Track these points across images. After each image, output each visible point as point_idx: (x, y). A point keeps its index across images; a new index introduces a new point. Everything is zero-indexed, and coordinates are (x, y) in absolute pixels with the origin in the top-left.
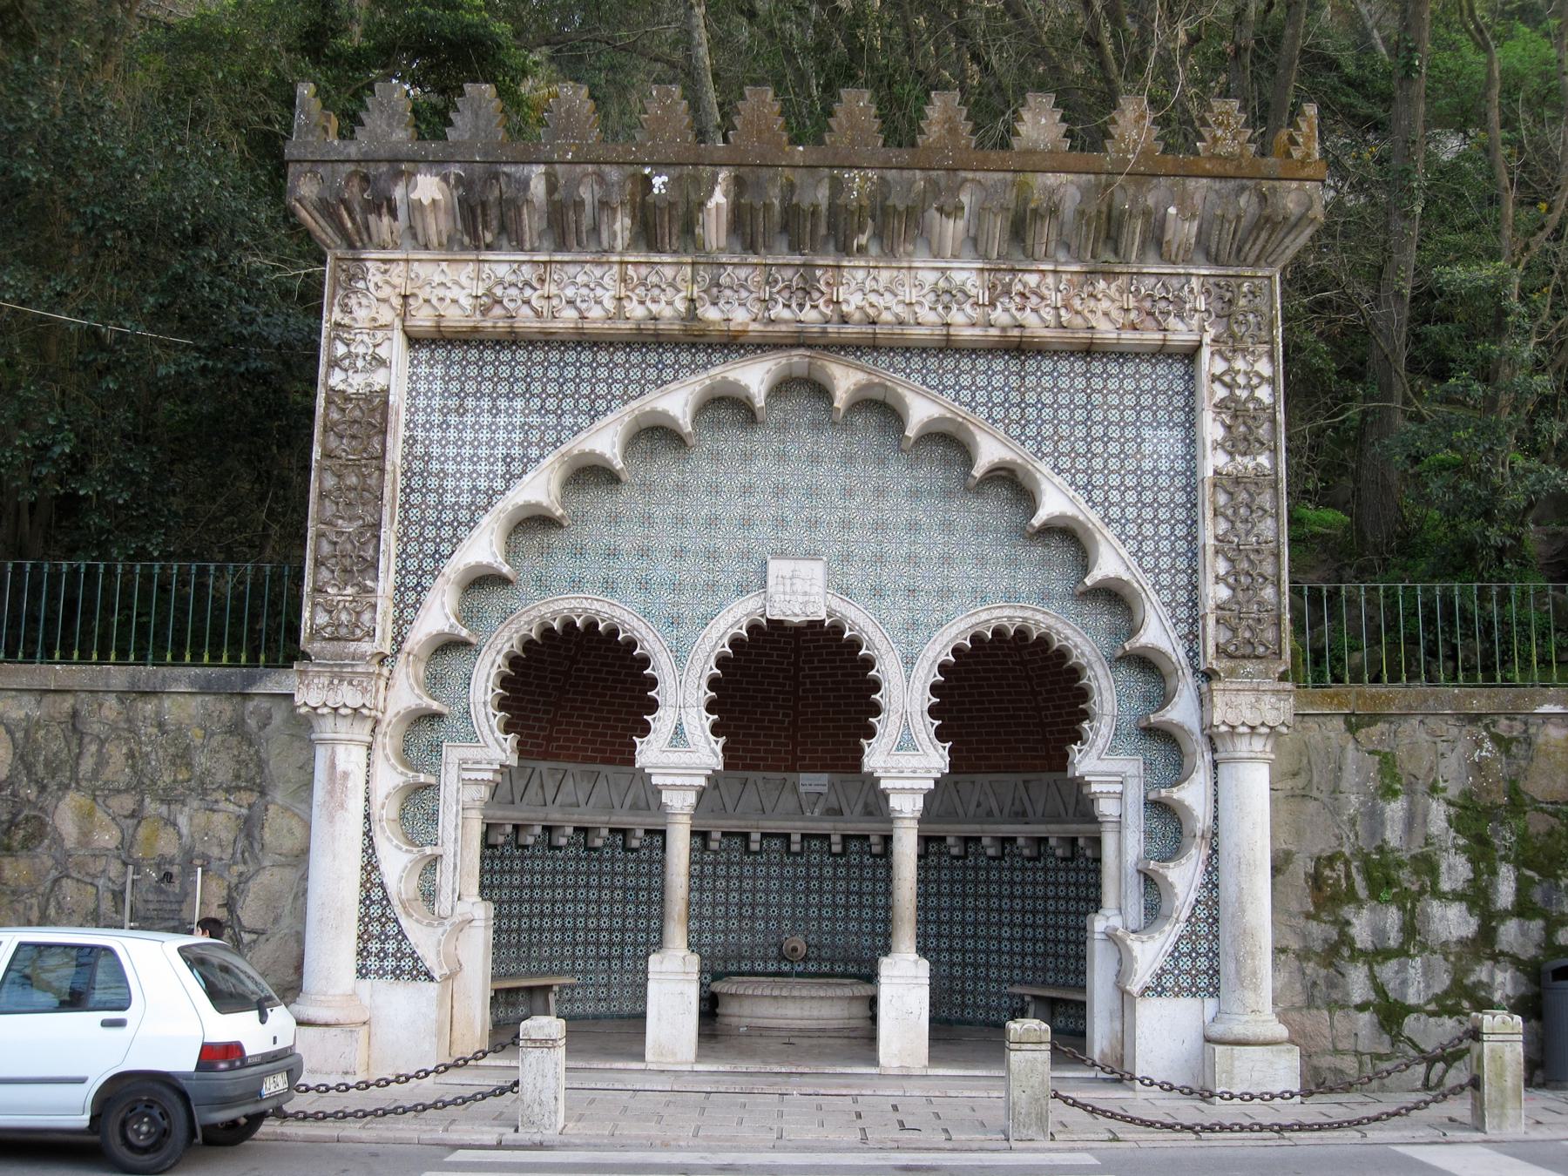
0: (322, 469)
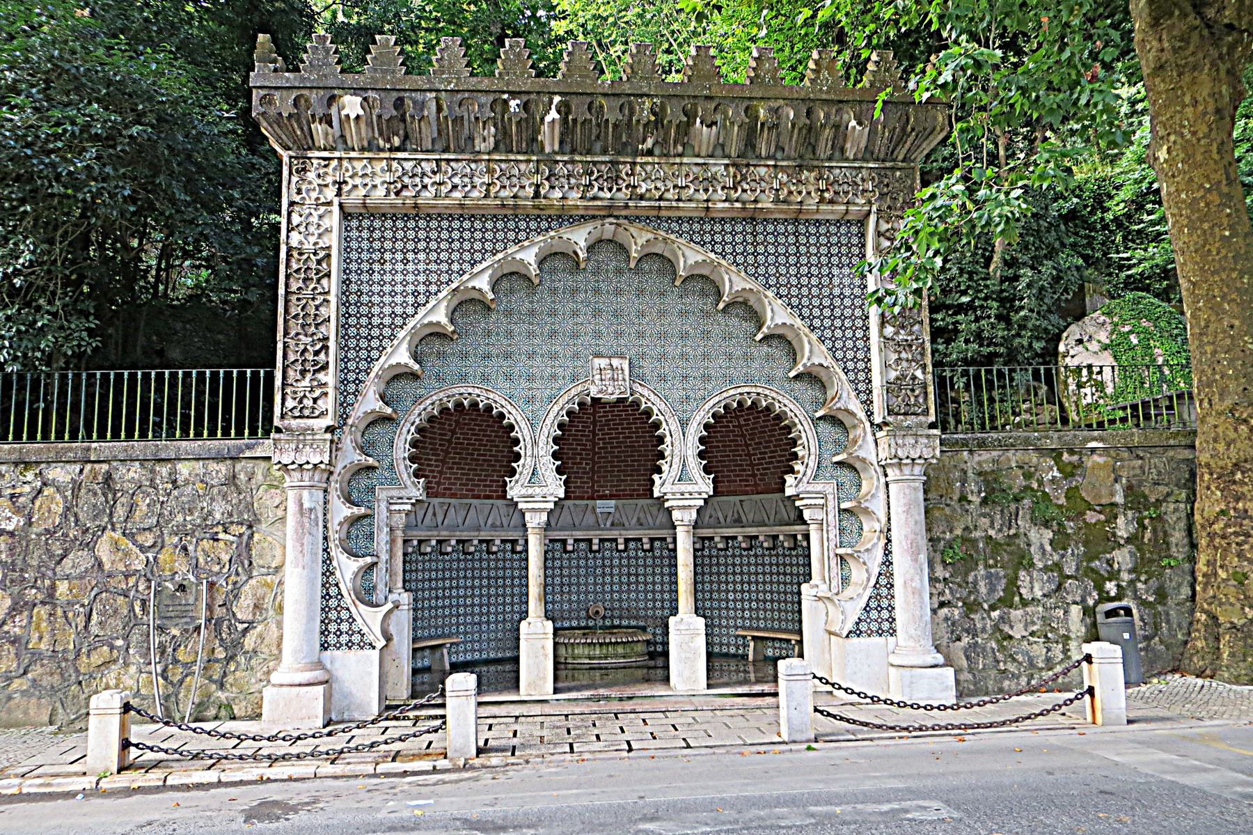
0: (287, 301)
